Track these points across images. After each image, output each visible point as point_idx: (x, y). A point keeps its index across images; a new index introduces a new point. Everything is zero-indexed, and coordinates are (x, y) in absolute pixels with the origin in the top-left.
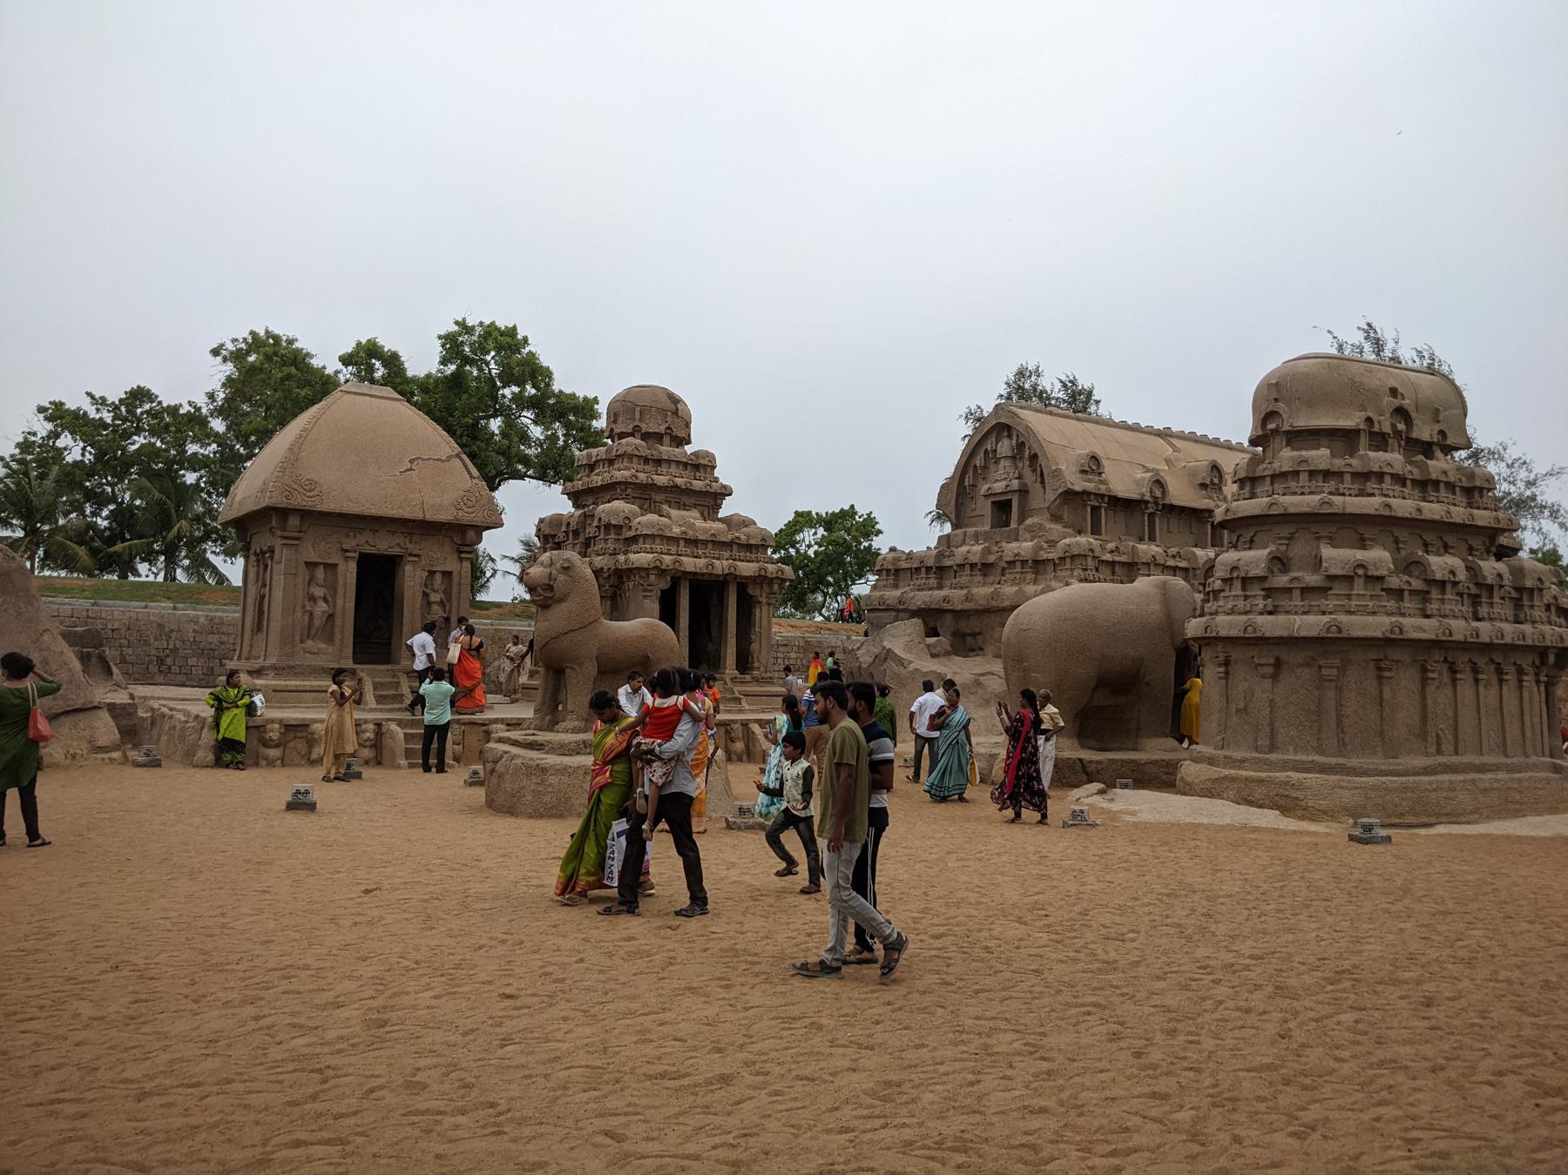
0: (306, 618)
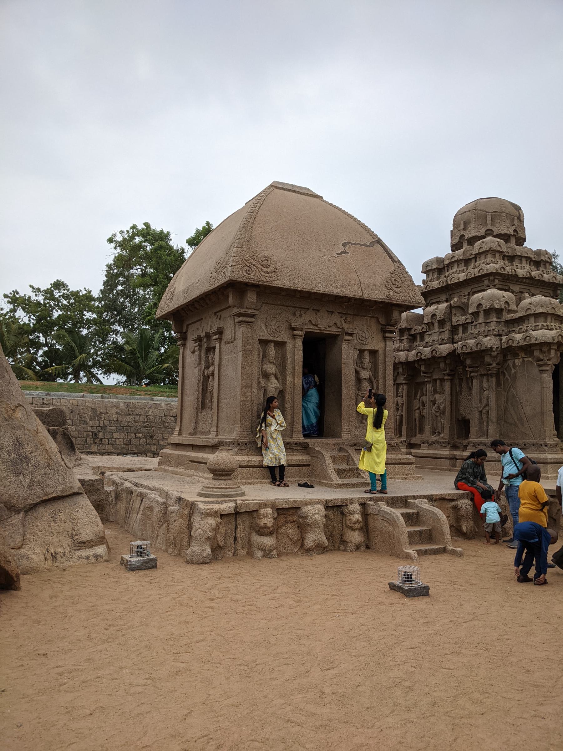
0: (262, 395)
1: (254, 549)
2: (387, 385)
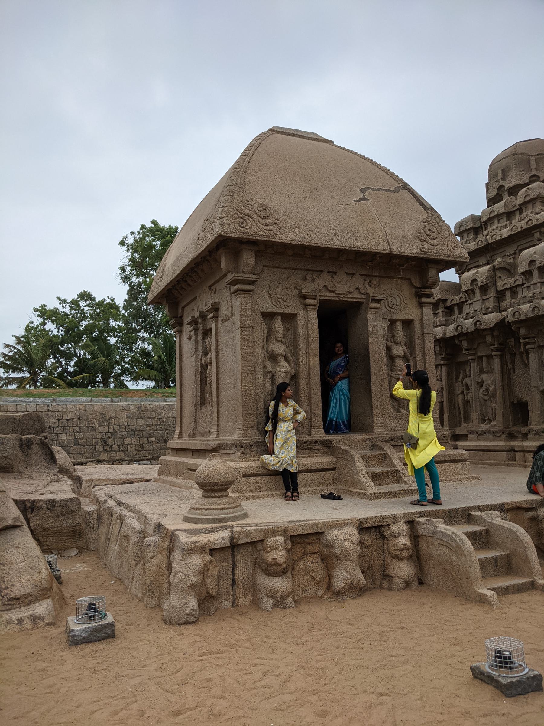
0: (269, 382)
1: (261, 596)
2: (427, 362)
